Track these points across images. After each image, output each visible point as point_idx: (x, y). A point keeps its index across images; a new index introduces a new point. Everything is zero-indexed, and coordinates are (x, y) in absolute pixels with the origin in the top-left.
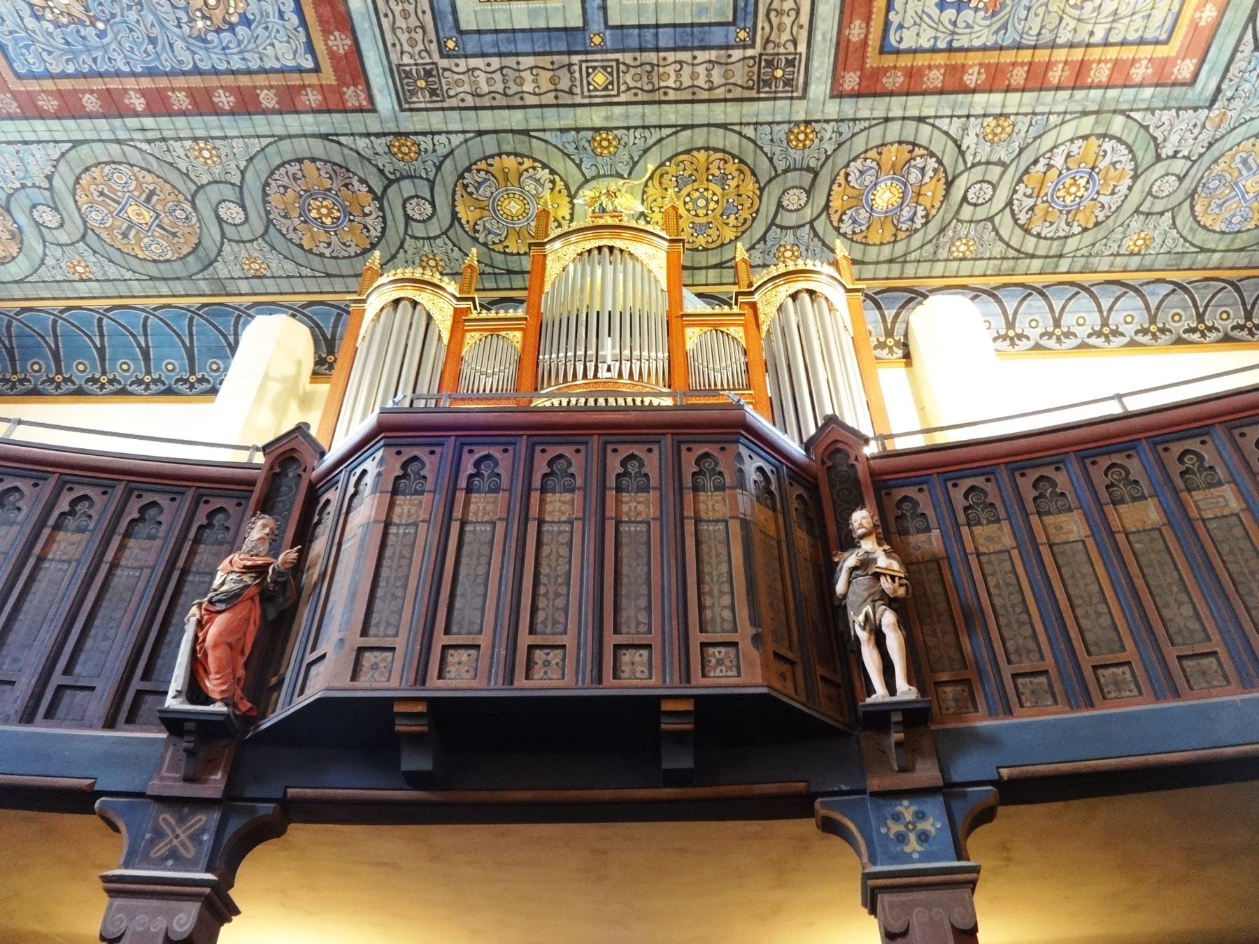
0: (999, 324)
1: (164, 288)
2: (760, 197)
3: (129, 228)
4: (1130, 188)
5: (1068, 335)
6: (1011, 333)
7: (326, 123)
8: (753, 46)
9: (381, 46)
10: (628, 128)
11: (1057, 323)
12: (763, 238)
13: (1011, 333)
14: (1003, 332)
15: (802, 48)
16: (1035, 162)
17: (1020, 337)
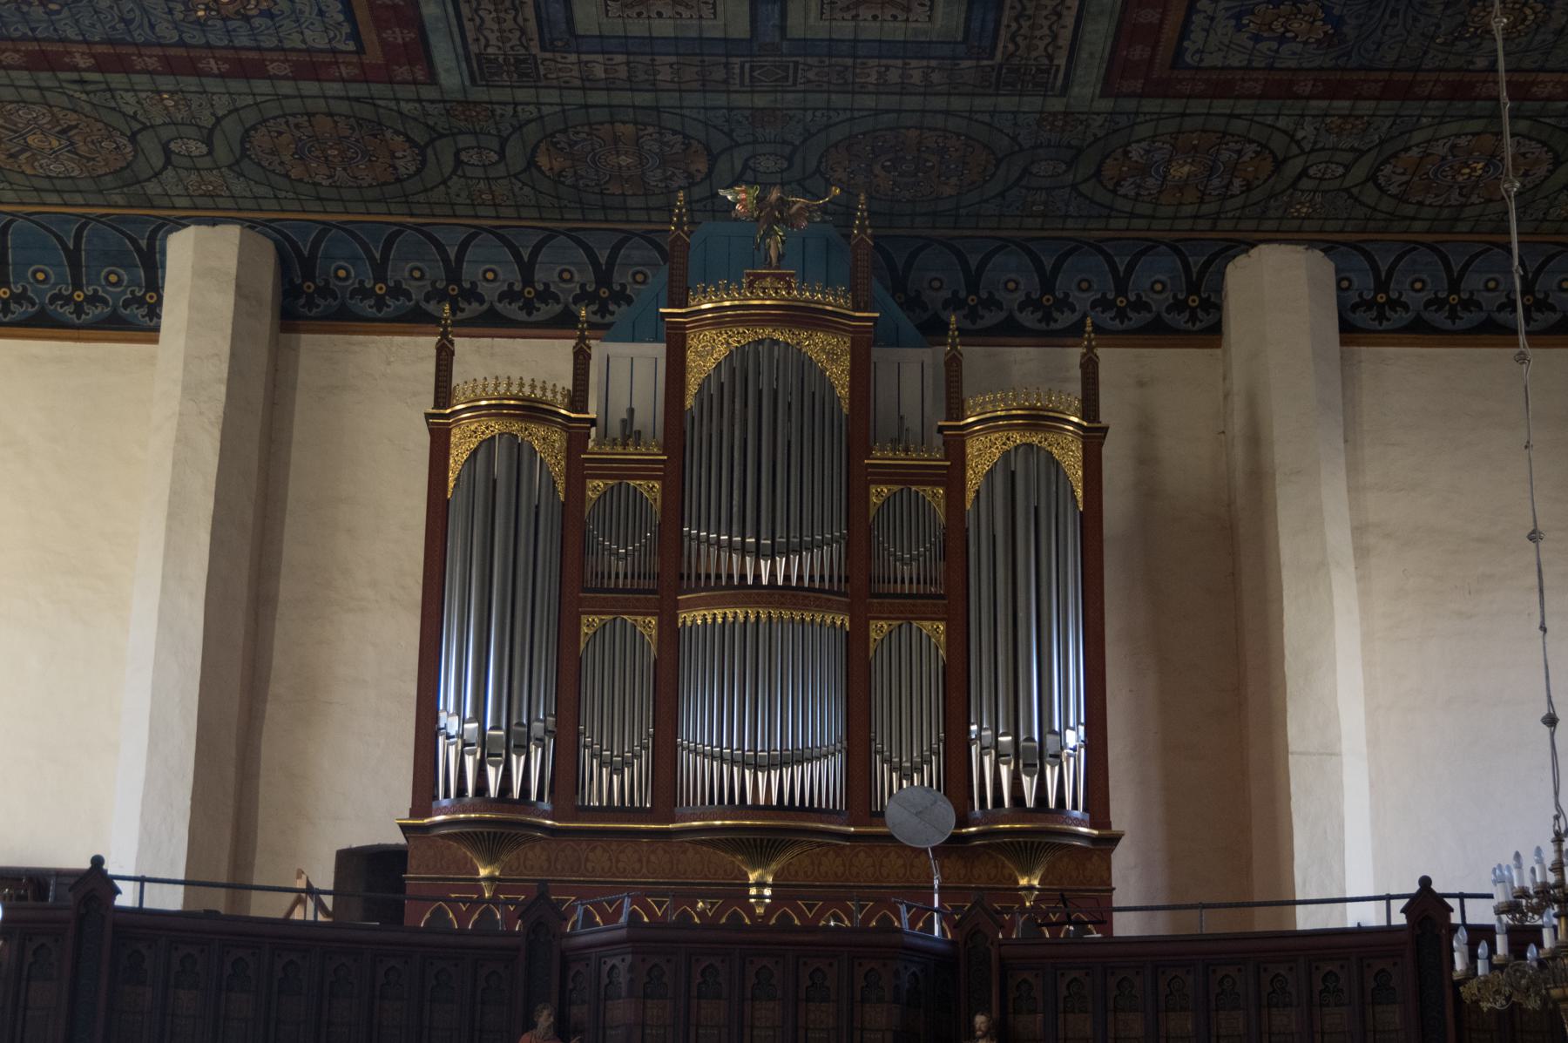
0: (1364, 282)
1: (54, 198)
2: (997, 167)
3: (22, 151)
4: (1551, 172)
5: (1469, 304)
6: (1381, 298)
7: (357, 90)
8: (992, 56)
9: (458, 39)
10: (805, 109)
11: (1454, 287)
12: (1002, 195)
13: (1381, 298)
14: (1368, 296)
15: (1061, 61)
16: (1407, 149)
17: (1394, 304)
